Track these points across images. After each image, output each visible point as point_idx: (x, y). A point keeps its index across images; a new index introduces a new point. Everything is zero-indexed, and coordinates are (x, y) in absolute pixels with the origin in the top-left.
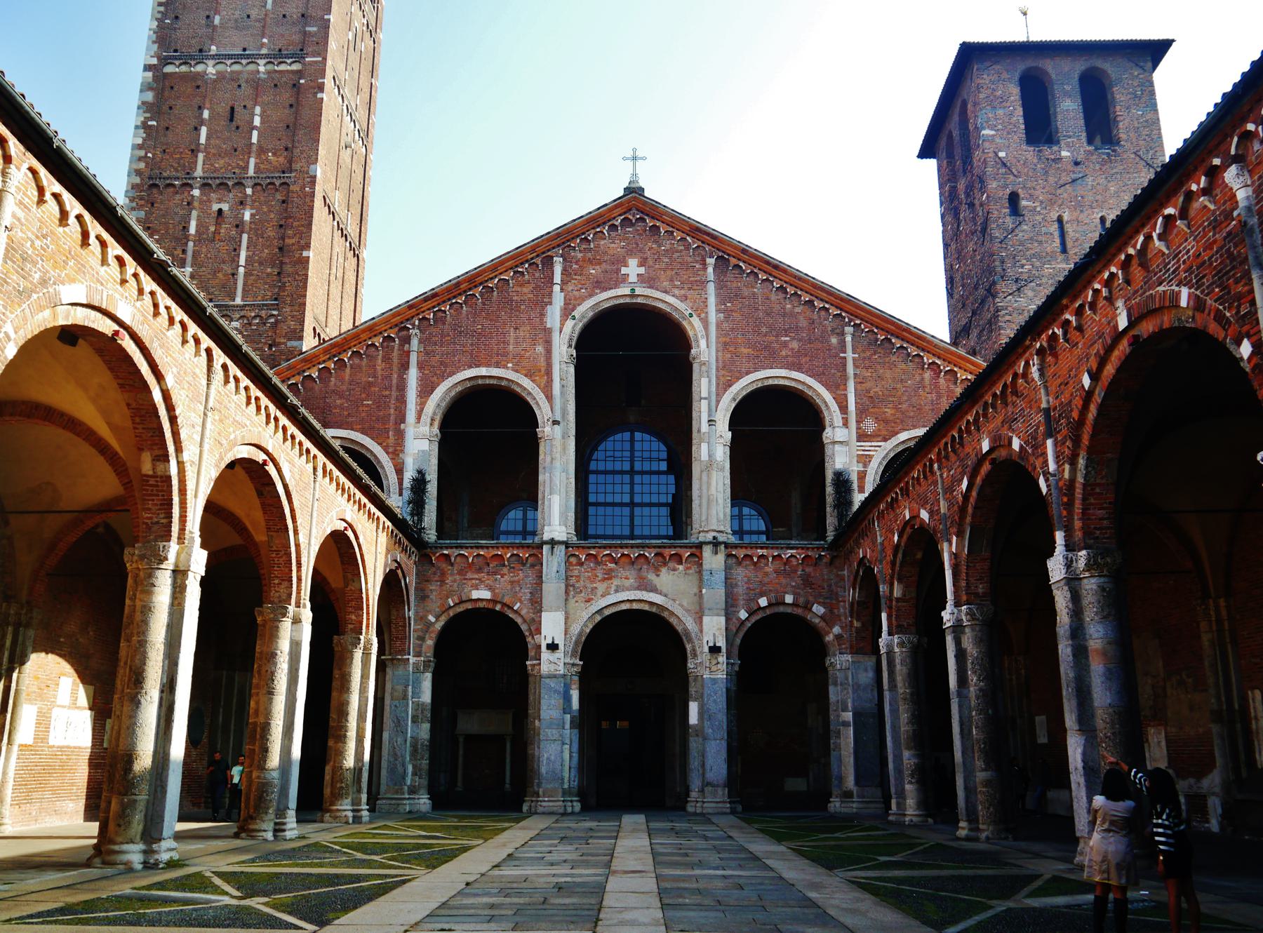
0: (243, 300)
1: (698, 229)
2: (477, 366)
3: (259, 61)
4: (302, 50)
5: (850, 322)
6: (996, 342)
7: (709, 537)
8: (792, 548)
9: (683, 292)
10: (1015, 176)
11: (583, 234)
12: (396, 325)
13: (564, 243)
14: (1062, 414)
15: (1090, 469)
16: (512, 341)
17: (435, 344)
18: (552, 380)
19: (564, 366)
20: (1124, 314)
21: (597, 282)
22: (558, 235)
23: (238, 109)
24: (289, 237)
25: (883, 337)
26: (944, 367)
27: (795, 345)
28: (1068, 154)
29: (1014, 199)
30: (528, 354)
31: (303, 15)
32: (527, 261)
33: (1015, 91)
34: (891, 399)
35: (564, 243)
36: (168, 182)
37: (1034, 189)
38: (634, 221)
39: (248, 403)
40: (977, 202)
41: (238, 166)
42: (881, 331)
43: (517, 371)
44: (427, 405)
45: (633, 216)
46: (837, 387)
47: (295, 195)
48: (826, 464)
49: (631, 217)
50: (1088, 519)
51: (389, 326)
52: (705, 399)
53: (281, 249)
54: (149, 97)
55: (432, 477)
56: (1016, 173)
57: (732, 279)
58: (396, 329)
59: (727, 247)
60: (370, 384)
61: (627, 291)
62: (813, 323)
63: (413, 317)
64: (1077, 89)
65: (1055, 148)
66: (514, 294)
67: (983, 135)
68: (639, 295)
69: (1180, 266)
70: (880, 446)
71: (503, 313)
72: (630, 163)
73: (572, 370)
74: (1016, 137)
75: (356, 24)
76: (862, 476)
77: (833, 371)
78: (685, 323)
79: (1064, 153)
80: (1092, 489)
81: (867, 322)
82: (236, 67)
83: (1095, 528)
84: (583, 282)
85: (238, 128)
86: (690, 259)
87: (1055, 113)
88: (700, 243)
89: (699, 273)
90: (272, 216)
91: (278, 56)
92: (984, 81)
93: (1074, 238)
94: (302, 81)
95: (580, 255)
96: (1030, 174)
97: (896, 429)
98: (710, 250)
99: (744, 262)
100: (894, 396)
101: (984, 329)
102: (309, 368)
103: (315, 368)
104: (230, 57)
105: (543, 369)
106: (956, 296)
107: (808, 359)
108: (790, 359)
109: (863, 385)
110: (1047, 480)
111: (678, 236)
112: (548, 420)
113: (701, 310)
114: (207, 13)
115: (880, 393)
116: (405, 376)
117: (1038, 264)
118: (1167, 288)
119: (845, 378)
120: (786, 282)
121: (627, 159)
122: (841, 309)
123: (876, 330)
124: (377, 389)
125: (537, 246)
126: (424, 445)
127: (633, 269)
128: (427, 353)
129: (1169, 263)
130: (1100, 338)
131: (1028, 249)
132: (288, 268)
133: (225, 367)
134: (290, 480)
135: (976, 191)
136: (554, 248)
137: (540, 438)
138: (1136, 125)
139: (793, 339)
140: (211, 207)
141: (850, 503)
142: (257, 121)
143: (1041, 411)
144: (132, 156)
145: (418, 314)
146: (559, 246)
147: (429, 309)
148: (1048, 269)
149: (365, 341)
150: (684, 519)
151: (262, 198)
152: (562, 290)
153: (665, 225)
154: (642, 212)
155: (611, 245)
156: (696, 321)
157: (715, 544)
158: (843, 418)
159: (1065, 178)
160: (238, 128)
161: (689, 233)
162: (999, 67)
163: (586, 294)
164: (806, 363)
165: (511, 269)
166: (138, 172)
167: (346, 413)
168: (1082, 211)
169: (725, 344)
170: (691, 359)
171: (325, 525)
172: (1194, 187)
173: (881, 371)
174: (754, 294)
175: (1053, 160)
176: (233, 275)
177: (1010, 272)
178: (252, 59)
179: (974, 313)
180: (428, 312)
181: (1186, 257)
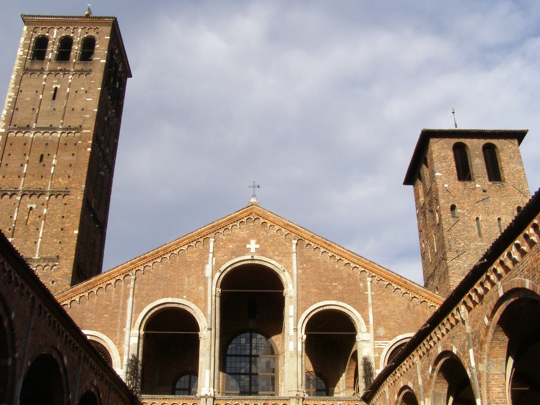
0: (39, 256)
1: (288, 225)
2: (167, 297)
3: (58, 131)
4: (81, 126)
5: (370, 275)
6: (447, 284)
7: (294, 394)
8: (340, 400)
9: (280, 258)
10: (453, 197)
11: (226, 226)
12: (123, 273)
13: (215, 231)
14: (476, 336)
15: (491, 366)
16: (186, 284)
17: (144, 284)
18: (208, 305)
19: (214, 298)
20: (501, 289)
21: (233, 252)
22: (213, 227)
23: (45, 156)
24: (67, 223)
25: (388, 283)
26: (420, 300)
27: (340, 287)
28: (479, 186)
29: (453, 208)
30: (195, 291)
31: (83, 109)
32: (195, 240)
33: (451, 154)
34: (393, 317)
35: (215, 231)
37: (463, 203)
38: (253, 220)
39: (50, 325)
40: (434, 209)
42: (386, 280)
43: (188, 300)
44: (138, 318)
45: (253, 217)
46: (362, 310)
47: (72, 201)
48: (358, 353)
49: (252, 218)
50: (493, 393)
51: (119, 274)
52: (292, 317)
53: (62, 229)
55: (140, 358)
56: (453, 195)
57: (306, 251)
58: (124, 275)
59: (303, 234)
60: (108, 306)
61: (249, 257)
62: (350, 275)
63: (132, 269)
64: (482, 152)
65: (473, 183)
66: (188, 258)
67: (436, 175)
68: (256, 260)
69: (524, 269)
70: (387, 343)
71: (182, 268)
72: (252, 189)
73: (218, 300)
74: (452, 177)
75: (109, 113)
76: (377, 360)
77: (361, 301)
78: (281, 275)
79: (477, 186)
80: (493, 377)
81: (379, 275)
83: (496, 398)
84: (226, 252)
85: (44, 165)
86: (283, 241)
87: (472, 165)
88: (289, 232)
89: (289, 248)
90: (58, 212)
91: (69, 129)
92: (435, 149)
93: (485, 230)
94: (80, 142)
95: (224, 238)
96: (461, 196)
97: (396, 334)
98: (294, 236)
99: (313, 242)
100: (394, 315)
101: (441, 277)
102: (74, 296)
103: (79, 296)
104: (43, 129)
105: (203, 299)
106: (426, 258)
107: (348, 295)
108: (338, 295)
109: (378, 309)
110: (470, 371)
112: (205, 328)
113: (288, 267)
114: (34, 107)
115: (387, 314)
116: (127, 302)
117: (467, 243)
118: (519, 279)
119: (367, 305)
120: (335, 253)
121: (251, 187)
122: (365, 268)
123: (383, 280)
124: (111, 308)
125: (202, 232)
126: (134, 340)
127: (253, 245)
128: (140, 289)
129: (519, 267)
130: (491, 299)
131: (462, 235)
132: (66, 239)
133: (40, 306)
134: (67, 364)
135: (433, 204)
136: (210, 233)
137: (200, 338)
138: (512, 172)
139: (339, 284)
140: (26, 206)
141: (371, 375)
142: (54, 162)
143: (465, 334)
145: (135, 268)
146: (213, 232)
147: (141, 265)
148: (472, 246)
149: (106, 282)
150: (280, 382)
151: (54, 202)
152: (214, 256)
153: (270, 222)
154: (258, 215)
155: (240, 231)
156: (286, 273)
157: (297, 398)
158: (367, 327)
159: (479, 198)
160: (44, 165)
161: (283, 226)
162: (442, 142)
163: (227, 259)
164: (347, 297)
165: (187, 244)
167: (93, 321)
168: (488, 215)
169: (303, 287)
170: (284, 294)
171: (83, 388)
172: (527, 232)
173: (387, 302)
174: (318, 259)
175: (472, 189)
176: (36, 243)
177: (453, 247)
179: (436, 268)
180: (141, 266)
181: (526, 264)
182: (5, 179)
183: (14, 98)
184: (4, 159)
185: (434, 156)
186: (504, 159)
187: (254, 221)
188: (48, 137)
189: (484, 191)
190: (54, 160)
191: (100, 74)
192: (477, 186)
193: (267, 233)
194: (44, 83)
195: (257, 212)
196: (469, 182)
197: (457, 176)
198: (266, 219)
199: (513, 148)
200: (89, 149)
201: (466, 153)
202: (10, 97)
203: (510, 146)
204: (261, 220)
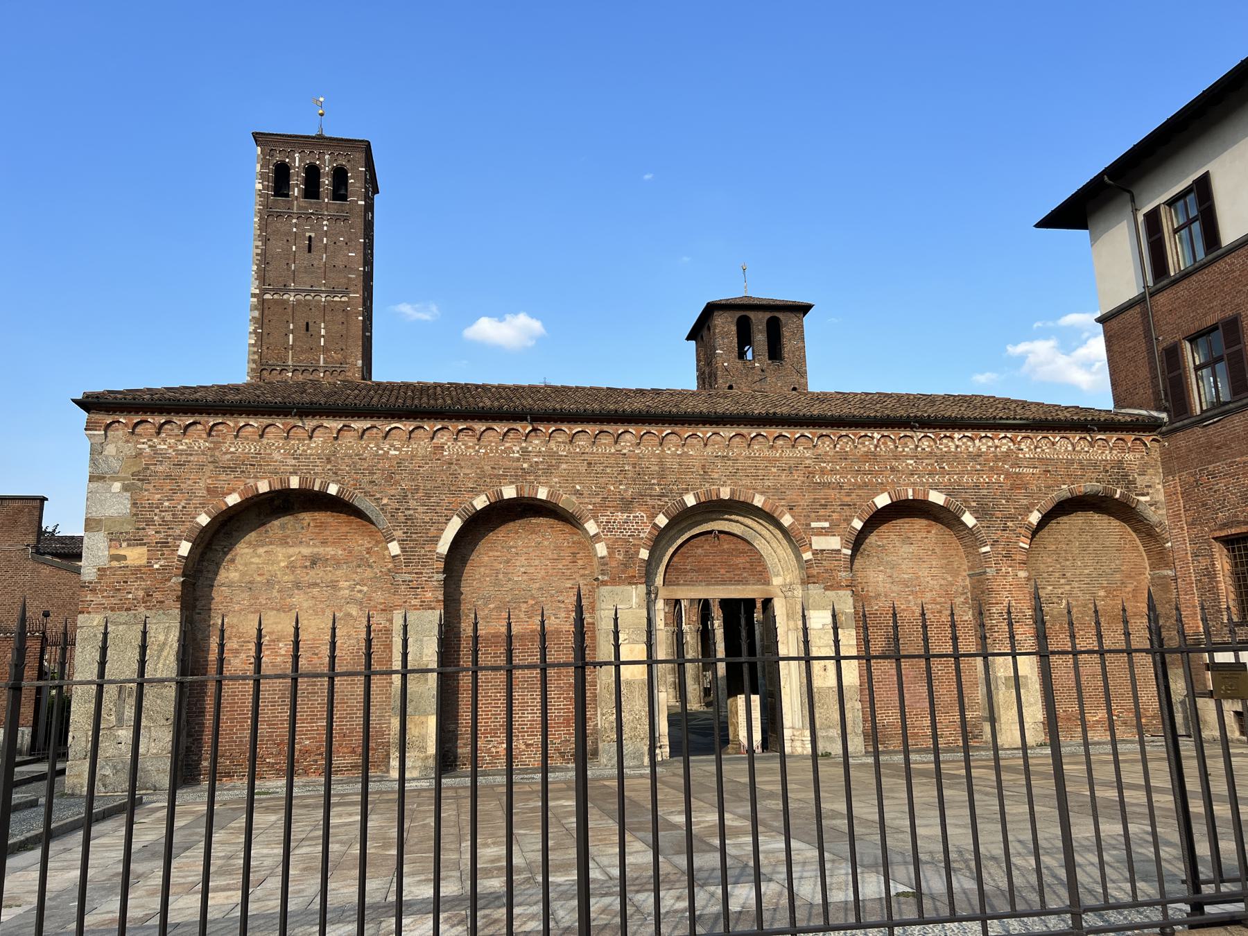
33: (734, 328)
36: (273, 367)
41: (314, 359)
54: (256, 314)
82: (308, 297)
104: (304, 291)
142: (323, 332)
144: (249, 351)
159: (756, 378)
166: (254, 361)
178: (318, 292)
182: (270, 352)
183: (262, 249)
184: (264, 326)
185: (717, 331)
188: (310, 300)
189: (763, 371)
190: (322, 330)
191: (359, 220)
192: (757, 365)
194: (295, 230)
200: (361, 318)
202: (257, 247)
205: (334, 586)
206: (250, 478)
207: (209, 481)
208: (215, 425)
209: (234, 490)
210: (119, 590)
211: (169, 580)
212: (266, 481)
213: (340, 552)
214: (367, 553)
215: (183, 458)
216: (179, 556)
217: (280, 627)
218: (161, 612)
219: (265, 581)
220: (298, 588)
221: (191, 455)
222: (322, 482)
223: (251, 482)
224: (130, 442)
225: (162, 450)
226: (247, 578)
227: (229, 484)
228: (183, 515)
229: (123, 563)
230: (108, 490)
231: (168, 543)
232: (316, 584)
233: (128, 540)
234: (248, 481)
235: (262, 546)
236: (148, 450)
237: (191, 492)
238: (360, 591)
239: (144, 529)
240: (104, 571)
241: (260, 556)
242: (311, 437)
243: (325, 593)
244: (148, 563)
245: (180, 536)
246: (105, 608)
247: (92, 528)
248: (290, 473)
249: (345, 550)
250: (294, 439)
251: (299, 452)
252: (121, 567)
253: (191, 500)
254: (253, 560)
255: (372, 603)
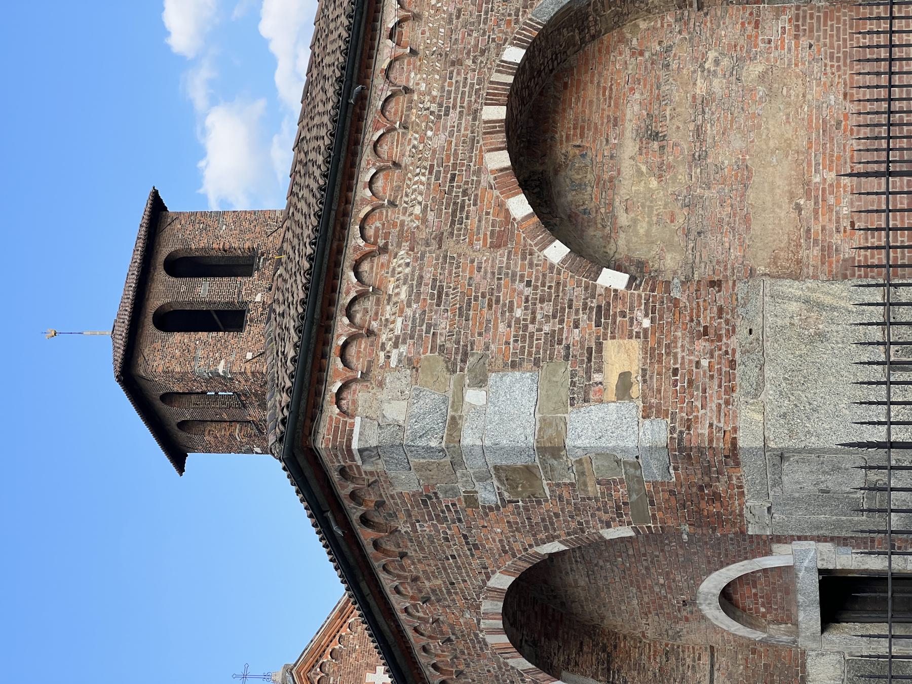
1: (342, 610)
28: (260, 295)
33: (177, 337)
45: (318, 674)
49: (319, 677)
65: (251, 306)
79: (258, 298)
87: (210, 303)
111: (346, 631)
161: (343, 620)
162: (146, 350)
185: (178, 369)
186: (206, 241)
187: (327, 675)
192: (258, 298)
193: (354, 650)
195: (306, 666)
196: (249, 312)
197: (232, 333)
198: (324, 651)
199: (183, 222)
201: (175, 311)
203: (180, 226)
204: (325, 660)
205: (702, 104)
206: (479, 182)
207: (479, 245)
208: (363, 236)
209: (501, 205)
210: (690, 382)
211: (676, 302)
212: (488, 156)
213: (637, 96)
214: (641, 54)
215: (426, 290)
216: (629, 286)
217: (779, 182)
218: (740, 310)
219: (685, 211)
220: (701, 158)
221: (421, 277)
222: (497, 71)
223: (486, 179)
224: (384, 379)
225: (404, 328)
226: (679, 239)
227: (488, 213)
228: (543, 285)
229: (635, 377)
230: (480, 411)
231: (599, 307)
232: (699, 131)
233: (588, 372)
234: (484, 184)
235: (615, 217)
236: (403, 349)
237: (498, 274)
238: (717, 62)
239: (568, 347)
240: (651, 407)
241: (635, 221)
242: (407, 90)
243: (717, 115)
244: (638, 337)
245: (586, 288)
246: (727, 403)
247: (559, 433)
248: (474, 119)
249: (632, 89)
250: (408, 116)
251: (434, 107)
252: (645, 381)
253: (514, 274)
254: (642, 231)
255: (742, 42)
